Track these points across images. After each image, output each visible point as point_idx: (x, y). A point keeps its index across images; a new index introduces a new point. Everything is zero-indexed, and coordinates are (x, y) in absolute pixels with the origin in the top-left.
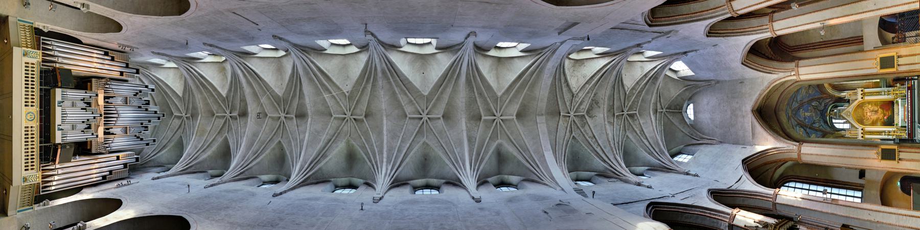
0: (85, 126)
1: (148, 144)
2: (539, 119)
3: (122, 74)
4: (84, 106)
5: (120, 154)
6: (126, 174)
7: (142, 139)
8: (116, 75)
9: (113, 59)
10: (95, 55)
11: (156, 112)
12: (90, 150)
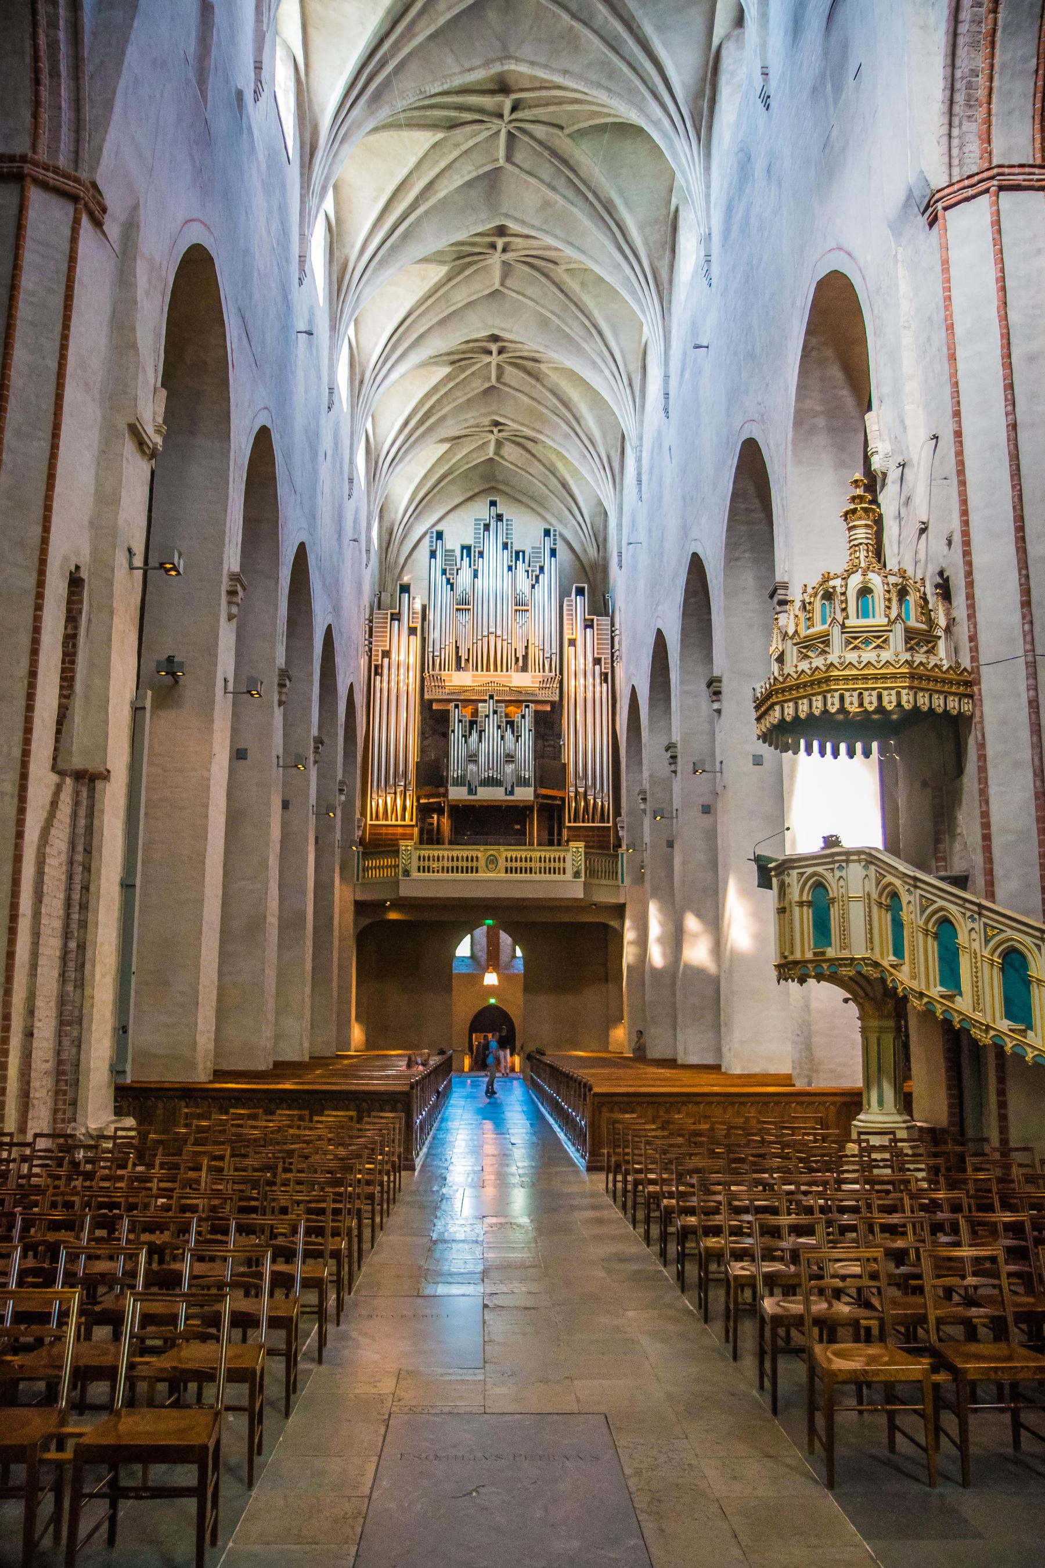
0: (508, 734)
2: (515, 1083)
3: (412, 631)
4: (475, 736)
5: (567, 637)
6: (606, 621)
7: (542, 569)
8: (415, 642)
9: (386, 654)
10: (385, 685)
11: (487, 527)
12: (553, 704)
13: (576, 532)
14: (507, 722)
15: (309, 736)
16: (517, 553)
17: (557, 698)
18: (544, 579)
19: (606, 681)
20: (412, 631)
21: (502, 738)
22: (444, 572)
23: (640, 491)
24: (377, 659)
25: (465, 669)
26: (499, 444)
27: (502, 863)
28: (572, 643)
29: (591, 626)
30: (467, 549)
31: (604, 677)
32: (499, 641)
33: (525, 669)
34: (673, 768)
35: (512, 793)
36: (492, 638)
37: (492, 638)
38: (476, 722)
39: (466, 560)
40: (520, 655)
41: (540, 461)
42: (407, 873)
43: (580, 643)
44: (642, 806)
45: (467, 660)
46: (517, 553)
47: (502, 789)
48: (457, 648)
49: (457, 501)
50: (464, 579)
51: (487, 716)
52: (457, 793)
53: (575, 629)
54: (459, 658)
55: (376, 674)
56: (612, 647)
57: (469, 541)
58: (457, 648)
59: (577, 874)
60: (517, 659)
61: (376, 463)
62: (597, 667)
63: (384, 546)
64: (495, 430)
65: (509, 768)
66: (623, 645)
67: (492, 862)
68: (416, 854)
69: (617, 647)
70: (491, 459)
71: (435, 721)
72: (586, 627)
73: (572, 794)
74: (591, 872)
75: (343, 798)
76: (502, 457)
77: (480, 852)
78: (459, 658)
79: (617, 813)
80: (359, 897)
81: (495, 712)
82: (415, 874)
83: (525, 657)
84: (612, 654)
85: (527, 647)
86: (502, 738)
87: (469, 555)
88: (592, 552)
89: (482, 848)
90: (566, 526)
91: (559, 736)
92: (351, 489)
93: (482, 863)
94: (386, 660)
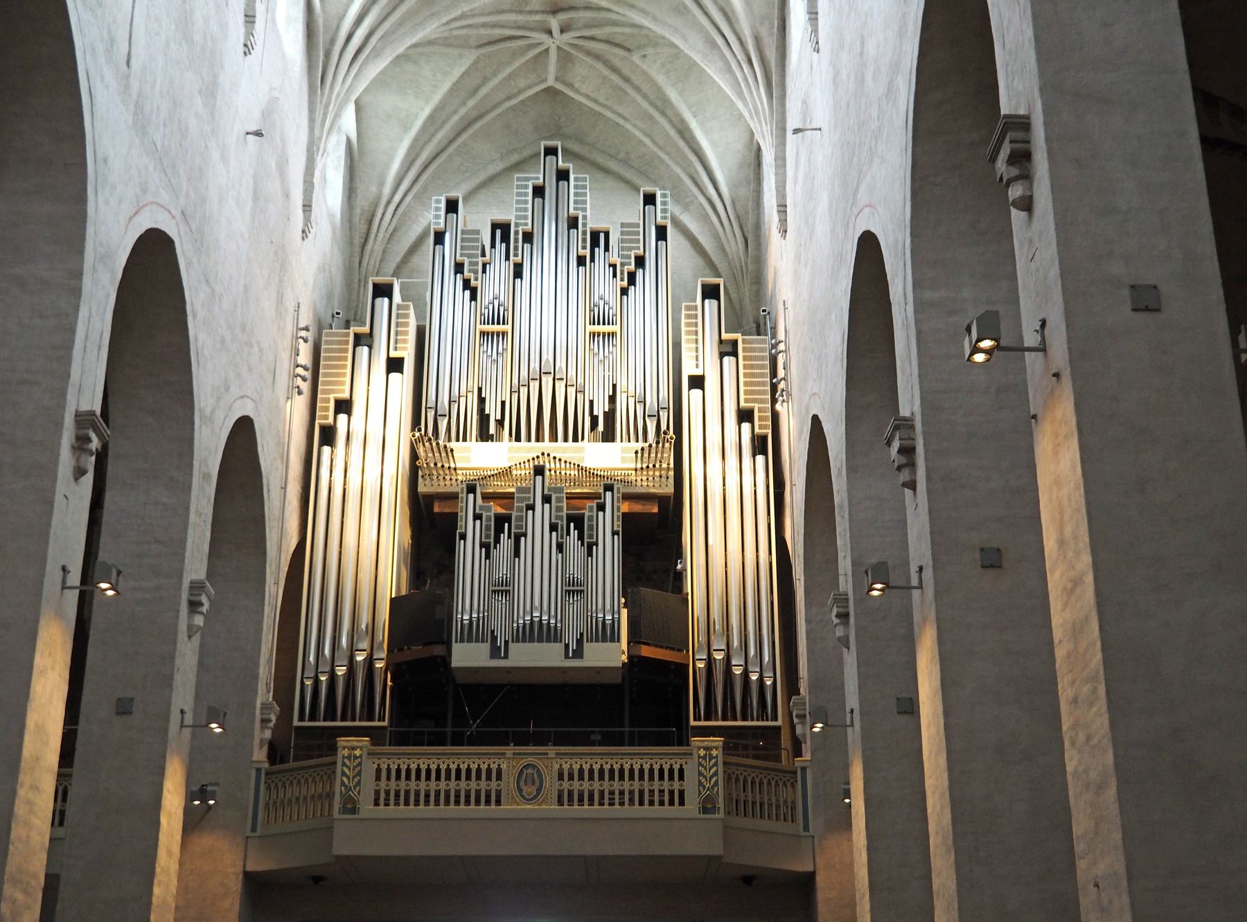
1: (661, 233)
3: (395, 365)
5: (689, 369)
7: (640, 262)
8: (402, 383)
9: (344, 406)
11: (539, 191)
13: (705, 217)
14: (570, 518)
15: (62, 406)
16: (595, 236)
17: (670, 489)
18: (646, 278)
19: (765, 453)
20: (395, 365)
21: (560, 547)
22: (459, 268)
23: (815, 30)
24: (326, 415)
25: (499, 439)
26: (565, 58)
27: (551, 785)
28: (697, 382)
29: (734, 354)
30: (502, 230)
31: (759, 445)
32: (560, 386)
33: (609, 436)
34: (905, 476)
35: (578, 654)
36: (547, 381)
37: (547, 381)
38: (508, 518)
39: (500, 247)
40: (599, 411)
41: (637, 89)
42: (351, 806)
43: (711, 383)
44: (840, 632)
45: (500, 423)
46: (595, 236)
47: (559, 647)
48: (482, 401)
49: (493, 169)
50: (495, 283)
51: (531, 507)
52: (467, 656)
53: (700, 357)
54: (484, 419)
55: (322, 444)
56: (774, 373)
57: (509, 216)
58: (482, 401)
59: (707, 806)
60: (594, 420)
61: (328, 54)
62: (746, 426)
63: (358, 241)
64: (554, 23)
65: (574, 608)
66: (793, 367)
67: (530, 781)
68: (369, 768)
69: (781, 373)
70: (550, 91)
71: (432, 525)
72: (722, 355)
73: (701, 665)
74: (737, 807)
75: (199, 620)
76: (570, 86)
77: (507, 760)
78: (484, 419)
79: (792, 686)
80: (251, 867)
81: (547, 499)
82: (367, 809)
83: (610, 416)
84: (774, 388)
85: (612, 399)
86: (560, 547)
87: (505, 238)
88: (735, 247)
89: (510, 750)
90: (686, 207)
91: (679, 554)
92: (249, 33)
93: (508, 784)
94: (342, 418)
